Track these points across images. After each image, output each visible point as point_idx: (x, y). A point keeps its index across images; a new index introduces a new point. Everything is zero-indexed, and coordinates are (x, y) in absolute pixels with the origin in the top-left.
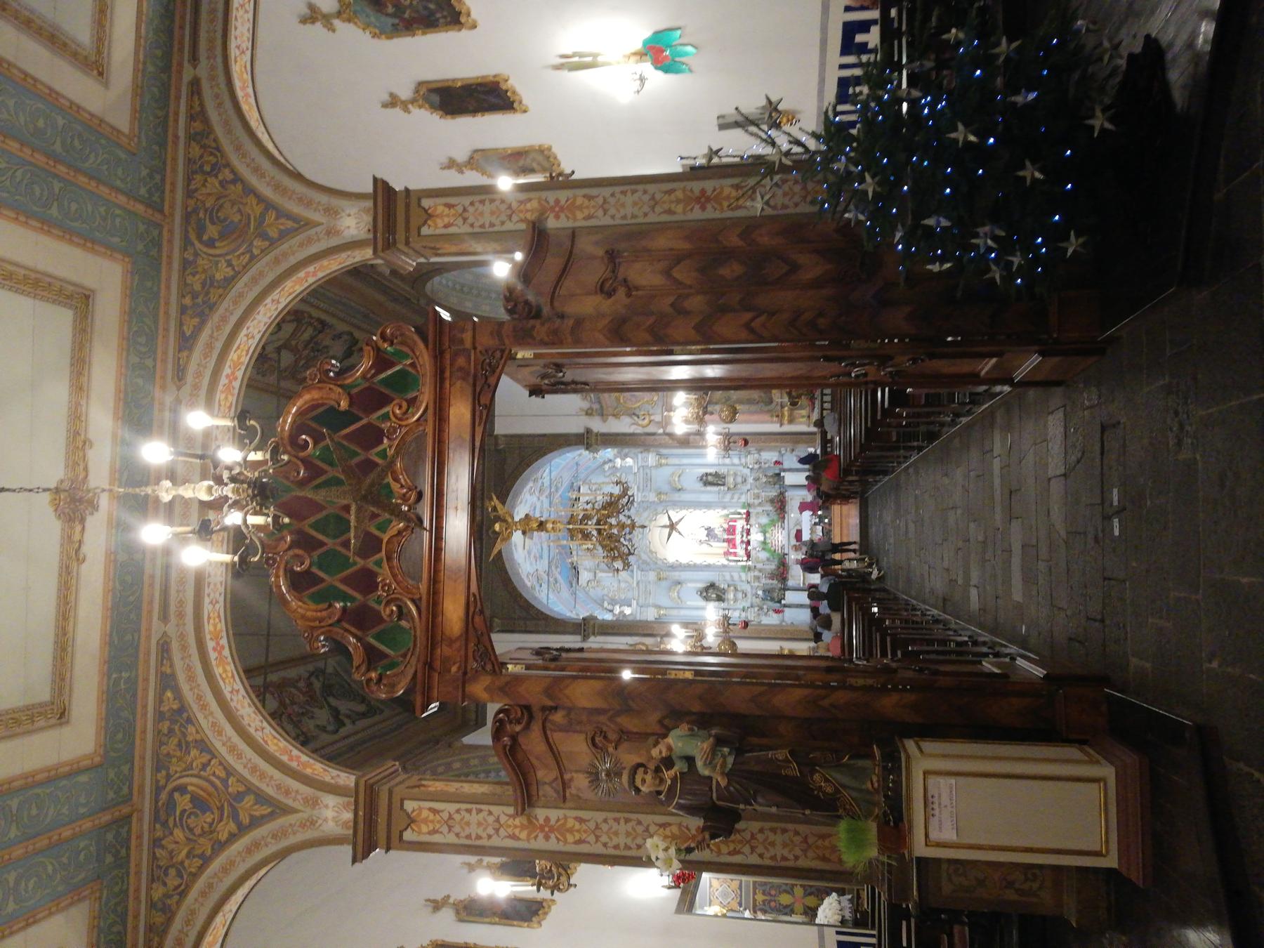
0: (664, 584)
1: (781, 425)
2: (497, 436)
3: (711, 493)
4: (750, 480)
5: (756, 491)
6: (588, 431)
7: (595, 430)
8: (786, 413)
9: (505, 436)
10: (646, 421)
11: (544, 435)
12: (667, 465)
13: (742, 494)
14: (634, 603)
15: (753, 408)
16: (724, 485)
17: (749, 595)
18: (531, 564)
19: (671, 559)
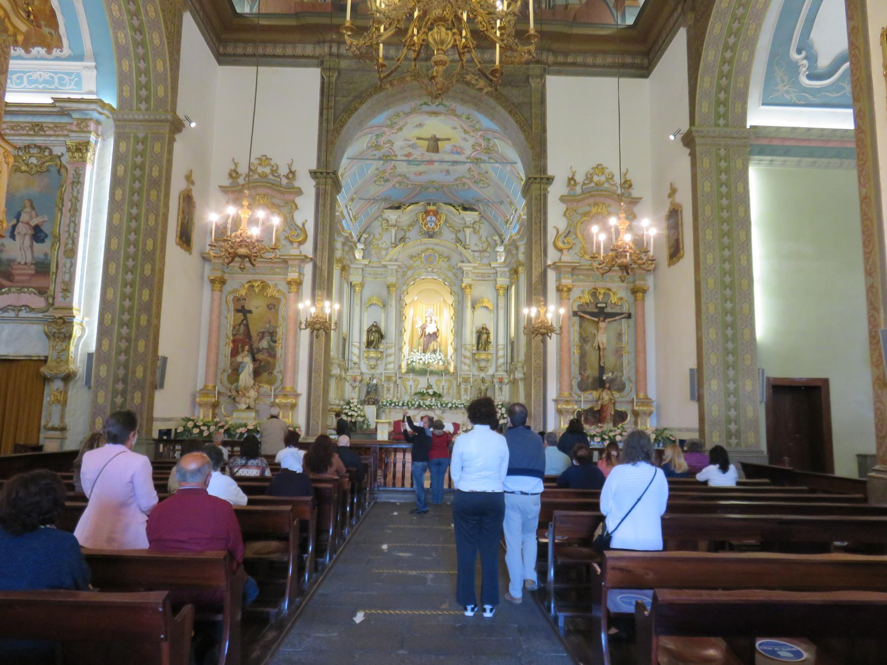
0: (384, 292)
1: (556, 401)
2: (542, 77)
3: (470, 338)
4: (482, 375)
5: (471, 379)
6: (550, 180)
7: (550, 189)
8: (570, 407)
9: (544, 86)
10: (560, 245)
11: (544, 130)
12: (498, 296)
13: (469, 366)
14: (366, 262)
15: (575, 370)
16: (478, 349)
17: (373, 371)
18: (402, 148)
19: (407, 299)
